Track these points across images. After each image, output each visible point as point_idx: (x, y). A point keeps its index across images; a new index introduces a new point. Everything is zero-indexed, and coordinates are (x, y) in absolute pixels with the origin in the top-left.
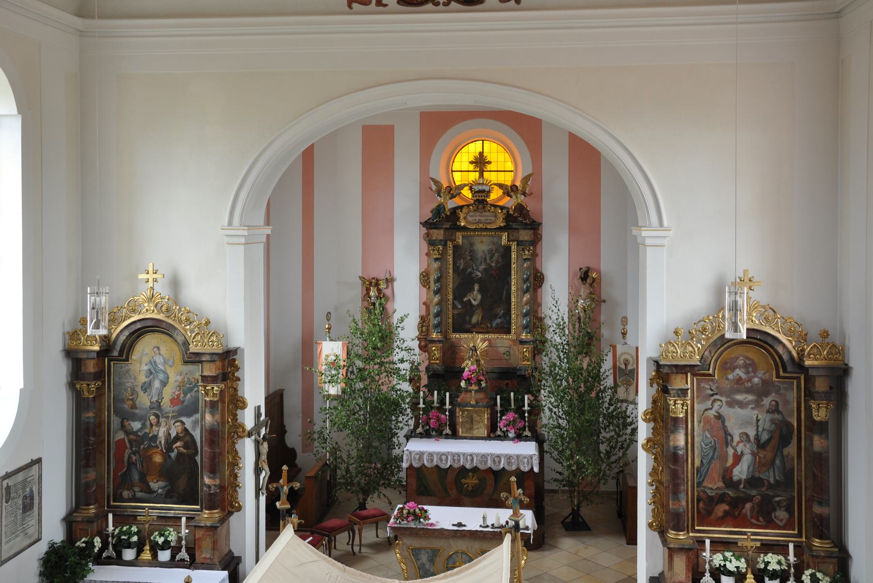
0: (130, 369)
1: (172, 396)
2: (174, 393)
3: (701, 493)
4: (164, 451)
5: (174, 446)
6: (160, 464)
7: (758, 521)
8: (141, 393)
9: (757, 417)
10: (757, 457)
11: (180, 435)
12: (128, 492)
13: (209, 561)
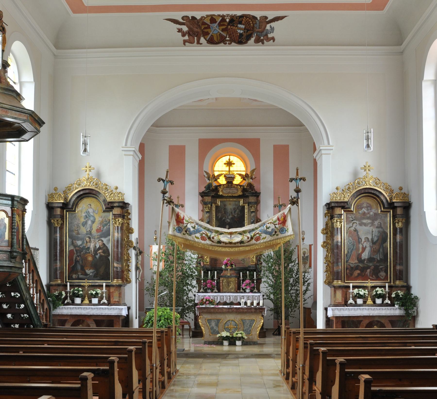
2: (98, 226)
3: (348, 265)
4: (93, 255)
5: (98, 252)
7: (373, 277)
8: (82, 227)
12: (76, 275)
13: (117, 303)
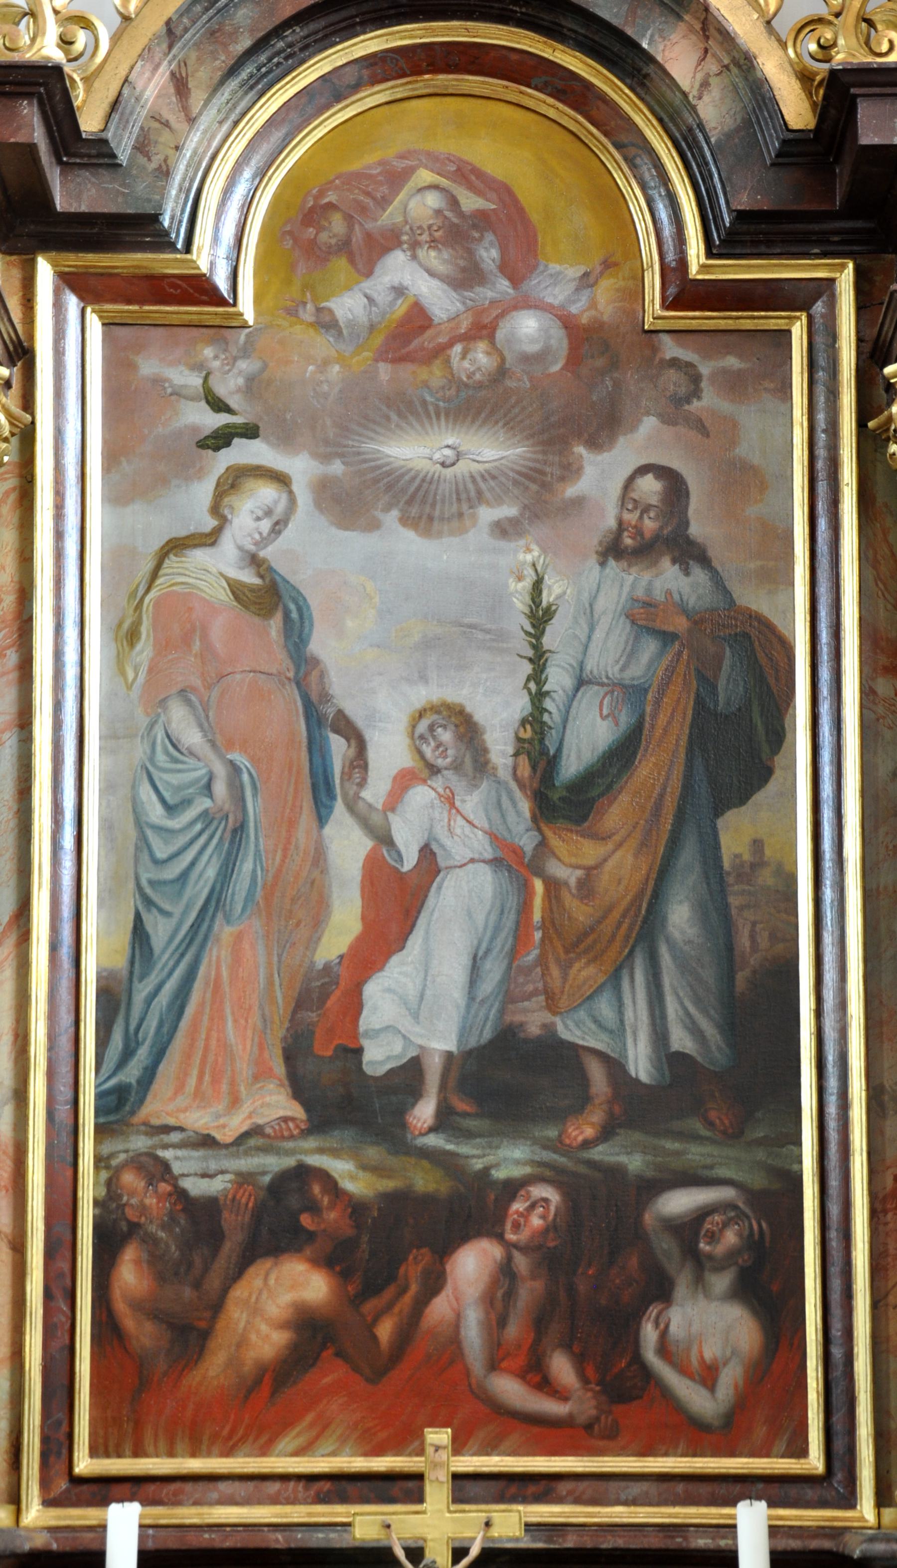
3: (129, 1178)
9: (537, 587)
10: (539, 886)
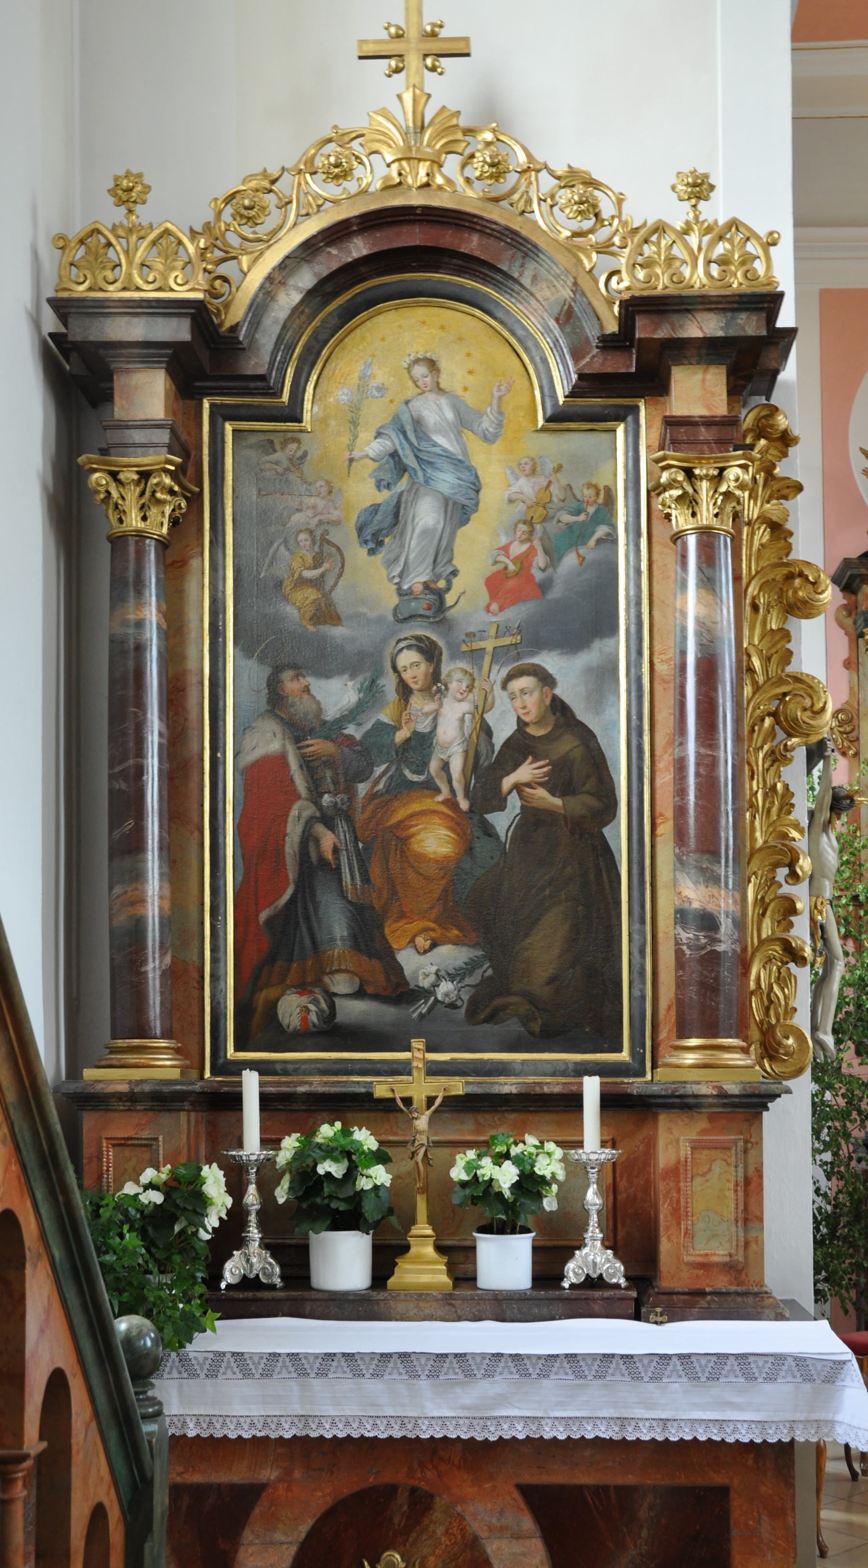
0: (305, 454)
1: (496, 562)
2: (505, 549)
4: (464, 805)
5: (507, 782)
6: (441, 863)
11: (532, 731)
12: (304, 1000)
13: (722, 1283)
